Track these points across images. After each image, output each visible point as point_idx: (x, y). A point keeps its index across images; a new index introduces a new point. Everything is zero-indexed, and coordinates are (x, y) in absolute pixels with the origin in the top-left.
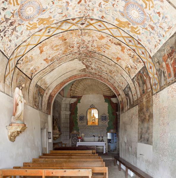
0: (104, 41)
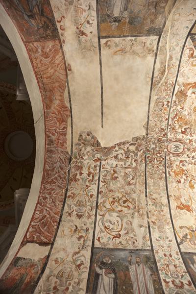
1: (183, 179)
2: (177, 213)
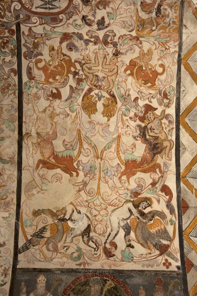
0: (131, 85)
1: (68, 88)
2: (37, 179)
